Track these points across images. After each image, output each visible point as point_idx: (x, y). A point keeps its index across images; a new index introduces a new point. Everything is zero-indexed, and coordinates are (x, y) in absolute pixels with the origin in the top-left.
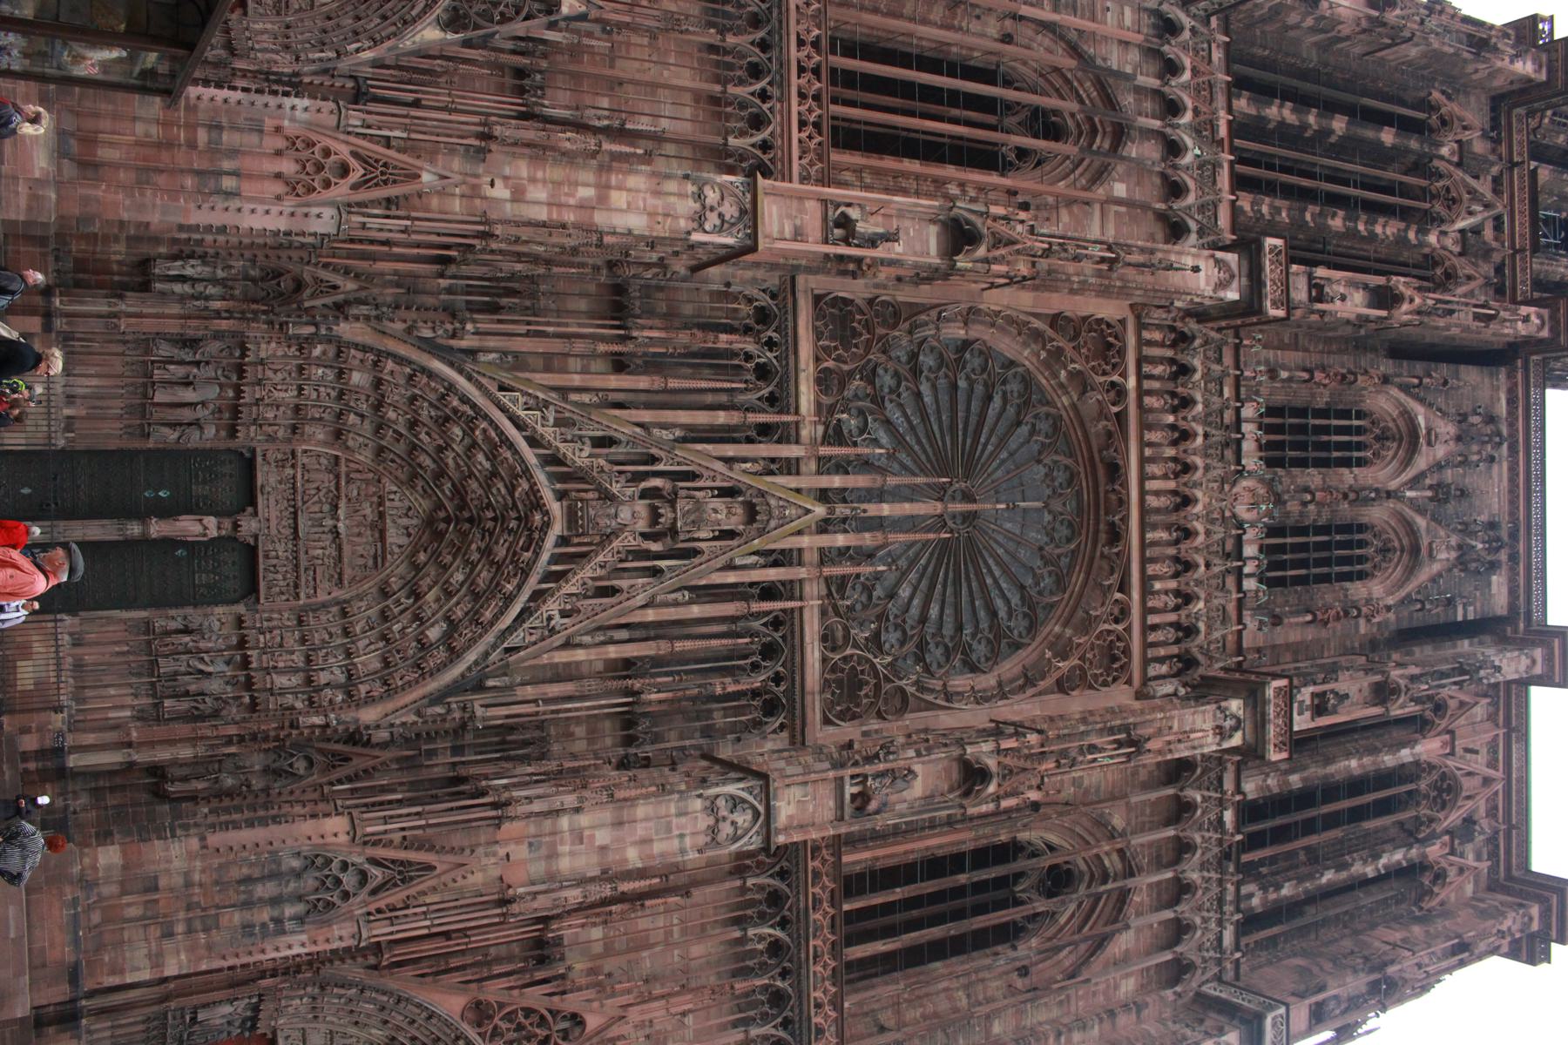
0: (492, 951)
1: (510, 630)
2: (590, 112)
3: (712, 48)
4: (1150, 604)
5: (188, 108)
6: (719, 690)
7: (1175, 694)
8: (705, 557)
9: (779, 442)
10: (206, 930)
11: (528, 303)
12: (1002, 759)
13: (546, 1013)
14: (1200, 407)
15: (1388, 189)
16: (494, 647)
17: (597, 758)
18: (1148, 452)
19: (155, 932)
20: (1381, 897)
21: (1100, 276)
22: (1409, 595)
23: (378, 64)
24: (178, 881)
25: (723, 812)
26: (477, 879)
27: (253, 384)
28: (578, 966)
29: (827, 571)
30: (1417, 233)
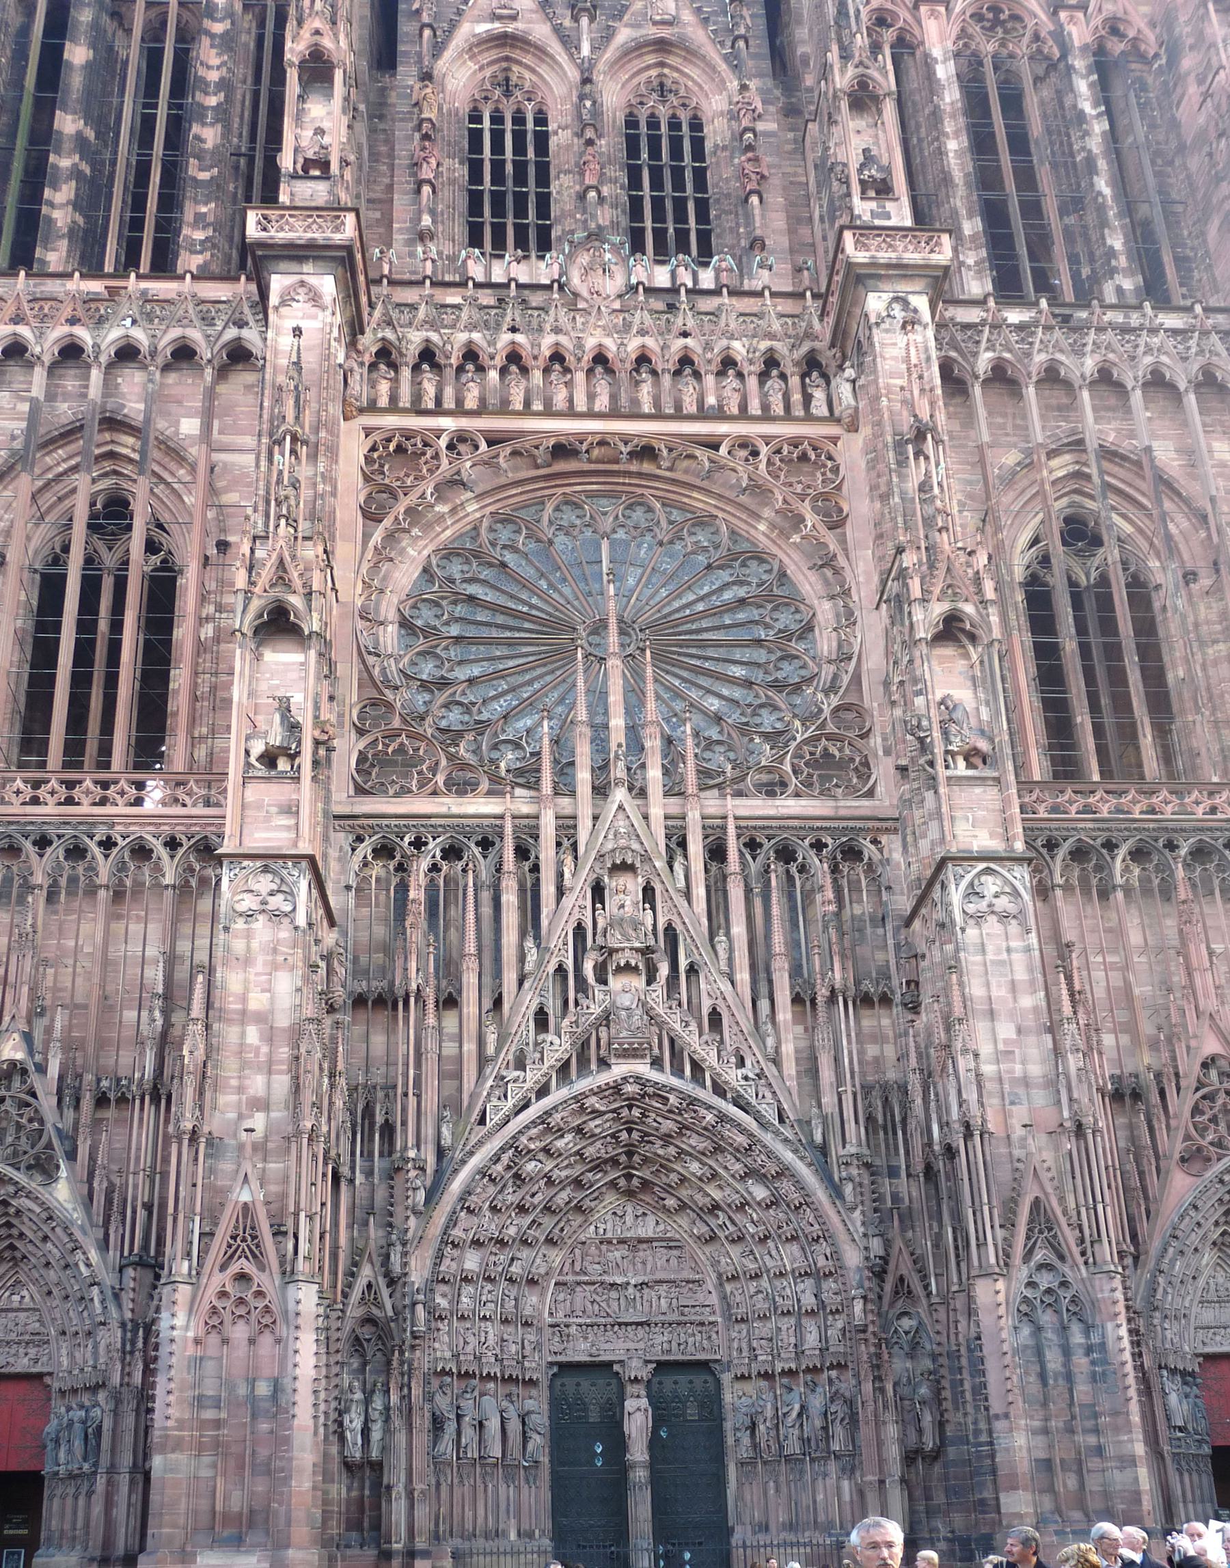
0: (1122, 1144)
1: (758, 1118)
2: (144, 1028)
3: (52, 897)
4: (735, 411)
7: (854, 381)
8: (675, 918)
9: (536, 837)
11: (380, 1094)
13: (1199, 1094)
14: (476, 336)
15: (153, 58)
16: (777, 1133)
17: (906, 1034)
18: (537, 406)
20: (1136, 115)
21: (316, 456)
22: (726, 58)
23: (104, 1245)
28: (1147, 1060)
29: (691, 789)
30: (214, 19)
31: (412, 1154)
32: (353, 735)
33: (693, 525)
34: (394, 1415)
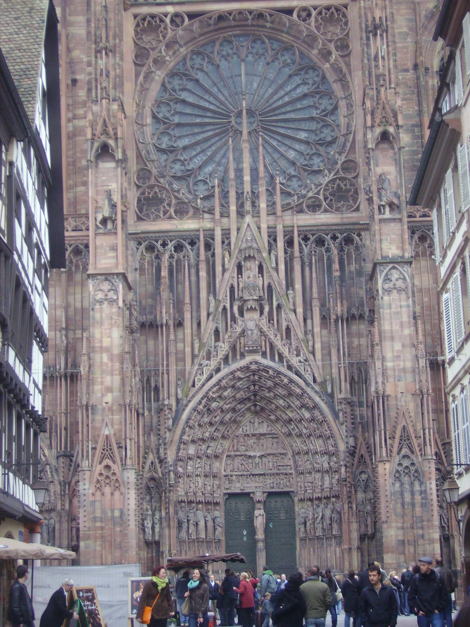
1: (305, 381)
5: (89, 530)
6: (337, 274)
9: (213, 239)
10: (422, 521)
11: (153, 373)
12: (376, 124)
16: (313, 388)
19: (421, 542)
23: (50, 447)
24: (400, 532)
25: (391, 285)
26: (411, 406)
27: (196, 497)
29: (279, 213)
31: (166, 402)
32: (135, 189)
33: (283, 50)
34: (163, 520)
